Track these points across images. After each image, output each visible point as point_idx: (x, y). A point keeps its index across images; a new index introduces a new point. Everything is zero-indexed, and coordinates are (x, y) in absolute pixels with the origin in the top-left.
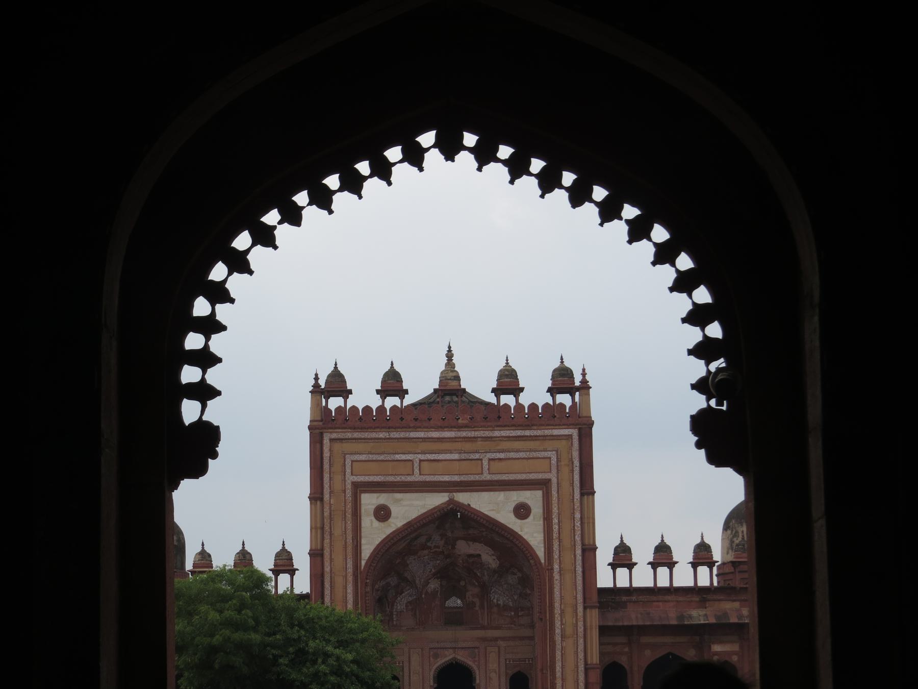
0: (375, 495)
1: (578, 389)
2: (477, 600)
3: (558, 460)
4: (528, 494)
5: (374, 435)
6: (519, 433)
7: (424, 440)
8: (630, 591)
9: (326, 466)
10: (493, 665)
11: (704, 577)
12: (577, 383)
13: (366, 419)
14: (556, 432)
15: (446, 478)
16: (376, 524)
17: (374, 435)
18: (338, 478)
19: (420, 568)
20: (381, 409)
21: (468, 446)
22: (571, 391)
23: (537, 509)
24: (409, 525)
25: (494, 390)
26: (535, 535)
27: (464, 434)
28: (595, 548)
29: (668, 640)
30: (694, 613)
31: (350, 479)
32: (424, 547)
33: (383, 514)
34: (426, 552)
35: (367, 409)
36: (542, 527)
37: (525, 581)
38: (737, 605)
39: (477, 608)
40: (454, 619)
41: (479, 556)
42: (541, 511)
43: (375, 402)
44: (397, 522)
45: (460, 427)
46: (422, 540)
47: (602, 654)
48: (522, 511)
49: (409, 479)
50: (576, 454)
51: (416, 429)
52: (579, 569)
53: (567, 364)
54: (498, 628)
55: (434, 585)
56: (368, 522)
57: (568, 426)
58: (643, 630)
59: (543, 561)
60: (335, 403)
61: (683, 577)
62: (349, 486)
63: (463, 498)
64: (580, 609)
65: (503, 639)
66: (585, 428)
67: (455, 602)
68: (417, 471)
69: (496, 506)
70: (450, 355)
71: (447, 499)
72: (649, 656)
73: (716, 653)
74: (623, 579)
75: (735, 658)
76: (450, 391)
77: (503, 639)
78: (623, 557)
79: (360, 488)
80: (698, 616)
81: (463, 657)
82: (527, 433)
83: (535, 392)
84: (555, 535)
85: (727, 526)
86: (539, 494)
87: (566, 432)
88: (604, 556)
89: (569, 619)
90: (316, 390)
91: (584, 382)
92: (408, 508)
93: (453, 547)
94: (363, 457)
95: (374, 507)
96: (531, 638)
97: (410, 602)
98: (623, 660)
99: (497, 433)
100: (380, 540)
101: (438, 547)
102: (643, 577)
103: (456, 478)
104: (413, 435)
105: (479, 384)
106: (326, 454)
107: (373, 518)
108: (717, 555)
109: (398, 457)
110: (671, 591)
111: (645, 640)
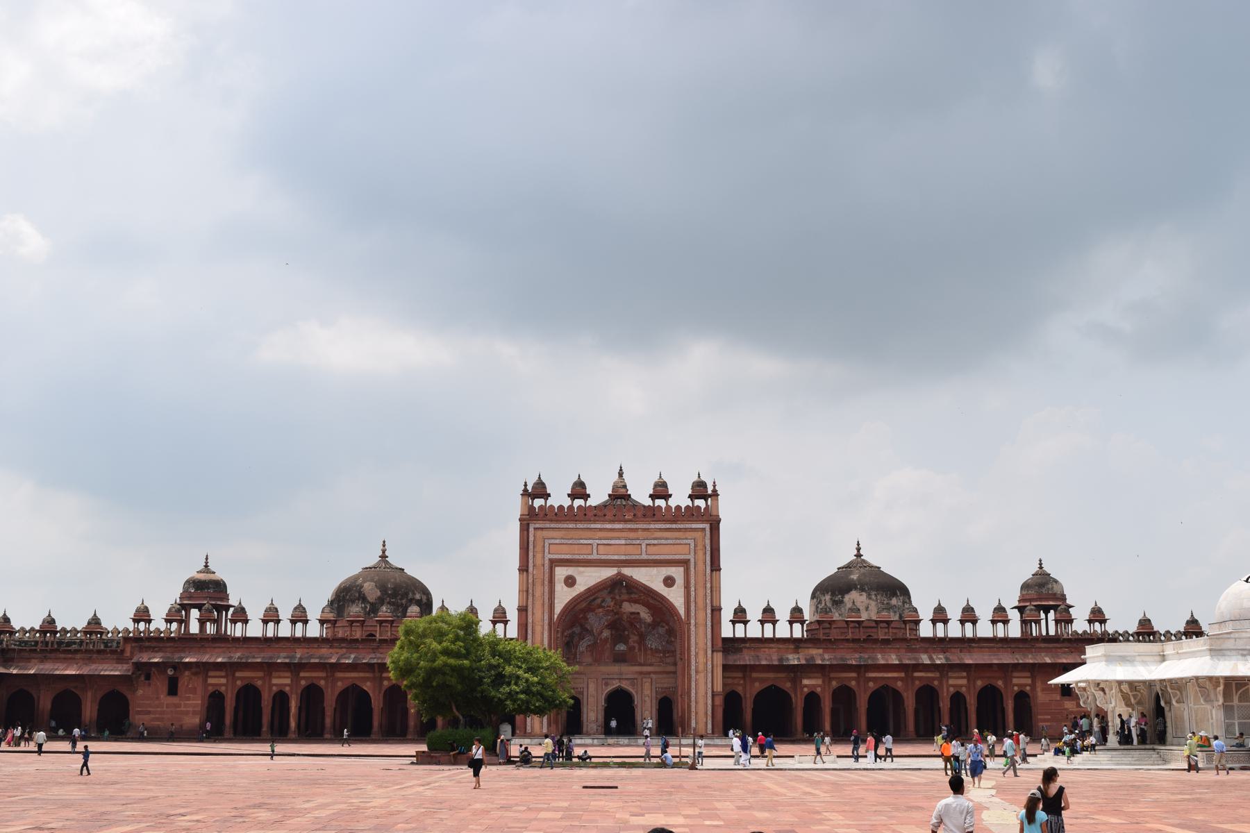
1: (710, 496)
3: (696, 546)
4: (673, 569)
5: (565, 526)
6: (668, 526)
7: (601, 530)
8: (745, 640)
9: (531, 547)
10: (647, 692)
11: (798, 631)
12: (710, 492)
13: (561, 515)
14: (694, 526)
15: (616, 557)
16: (566, 588)
17: (565, 526)
18: (539, 556)
19: (596, 622)
20: (571, 507)
21: (632, 535)
22: (705, 497)
23: (680, 581)
24: (589, 590)
25: (651, 496)
27: (629, 526)
28: (720, 609)
29: (771, 675)
30: (790, 656)
31: (548, 556)
32: (600, 606)
33: (570, 581)
35: (561, 507)
37: (671, 632)
38: (821, 651)
40: (620, 659)
43: (567, 502)
44: (580, 587)
45: (626, 521)
46: (599, 601)
47: (724, 685)
48: (669, 581)
49: (589, 557)
50: (708, 542)
51: (595, 522)
52: (709, 624)
53: (703, 478)
54: (651, 665)
55: (606, 633)
56: (560, 587)
57: (702, 522)
58: (753, 668)
60: (538, 503)
61: (783, 631)
62: (547, 562)
63: (627, 571)
64: (709, 652)
65: (655, 673)
66: (715, 524)
67: (621, 647)
69: (650, 578)
70: (621, 474)
72: (758, 687)
73: (806, 686)
74: (740, 631)
75: (819, 690)
76: (620, 495)
77: (655, 673)
78: (740, 616)
79: (554, 563)
80: (793, 659)
81: (626, 685)
82: (674, 526)
83: (680, 497)
84: (692, 599)
85: (813, 596)
86: (682, 569)
87: (701, 526)
88: (727, 615)
89: (701, 659)
90: (525, 493)
91: (715, 491)
92: (588, 578)
96: (675, 673)
98: (740, 690)
99: (652, 526)
102: (754, 631)
103: (623, 558)
104: (593, 526)
105: (641, 494)
106: (531, 539)
108: (807, 616)
110: (774, 640)
111: (755, 675)
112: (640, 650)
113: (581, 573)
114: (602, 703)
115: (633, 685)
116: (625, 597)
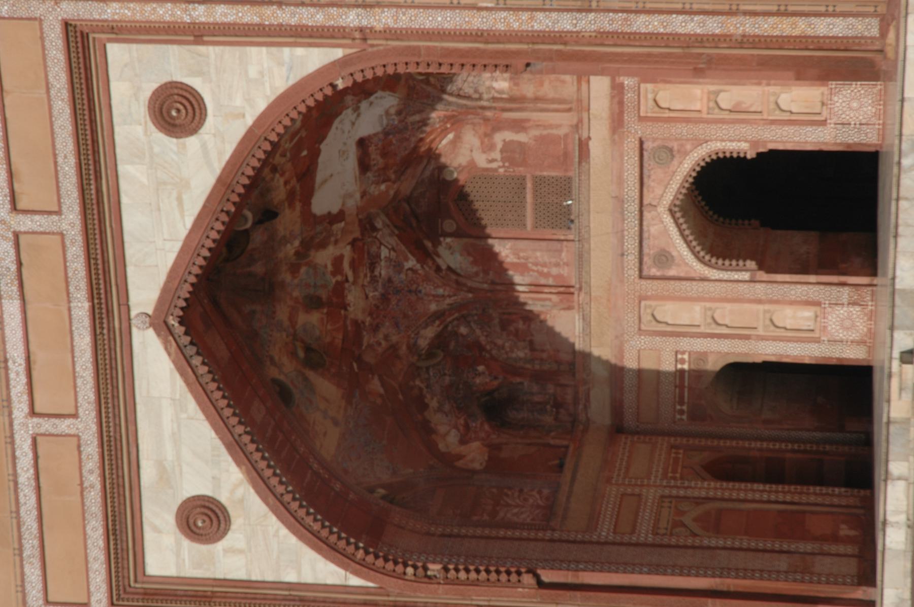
0: (149, 536)
2: (500, 138)
15: (84, 341)
16: (234, 538)
23: (174, 63)
24: (236, 448)
26: (253, 72)
32: (335, 303)
33: (204, 519)
34: (353, 297)
36: (227, 49)
39: (522, 137)
41: (362, 143)
42: (175, 48)
48: (177, 110)
49: (91, 449)
59: (339, 53)
68: (64, 426)
71: (151, 332)
86: (118, 54)
93: (340, 216)
94: (33, 573)
95: (186, 543)
97: (504, 325)
100: (284, 531)
101: (338, 261)
103: (81, 309)
107: (220, 546)
109: (25, 476)
112: (518, 126)
113: (165, 476)
114: (740, 276)
115: (669, 153)
116: (289, 221)
